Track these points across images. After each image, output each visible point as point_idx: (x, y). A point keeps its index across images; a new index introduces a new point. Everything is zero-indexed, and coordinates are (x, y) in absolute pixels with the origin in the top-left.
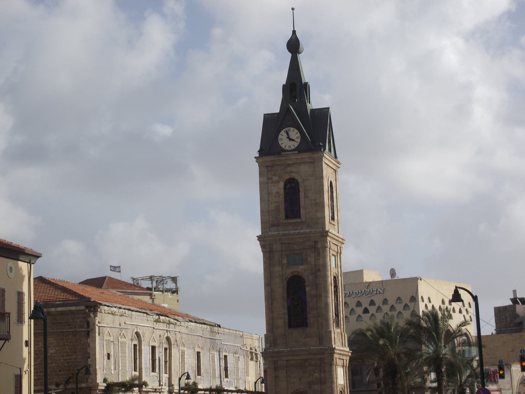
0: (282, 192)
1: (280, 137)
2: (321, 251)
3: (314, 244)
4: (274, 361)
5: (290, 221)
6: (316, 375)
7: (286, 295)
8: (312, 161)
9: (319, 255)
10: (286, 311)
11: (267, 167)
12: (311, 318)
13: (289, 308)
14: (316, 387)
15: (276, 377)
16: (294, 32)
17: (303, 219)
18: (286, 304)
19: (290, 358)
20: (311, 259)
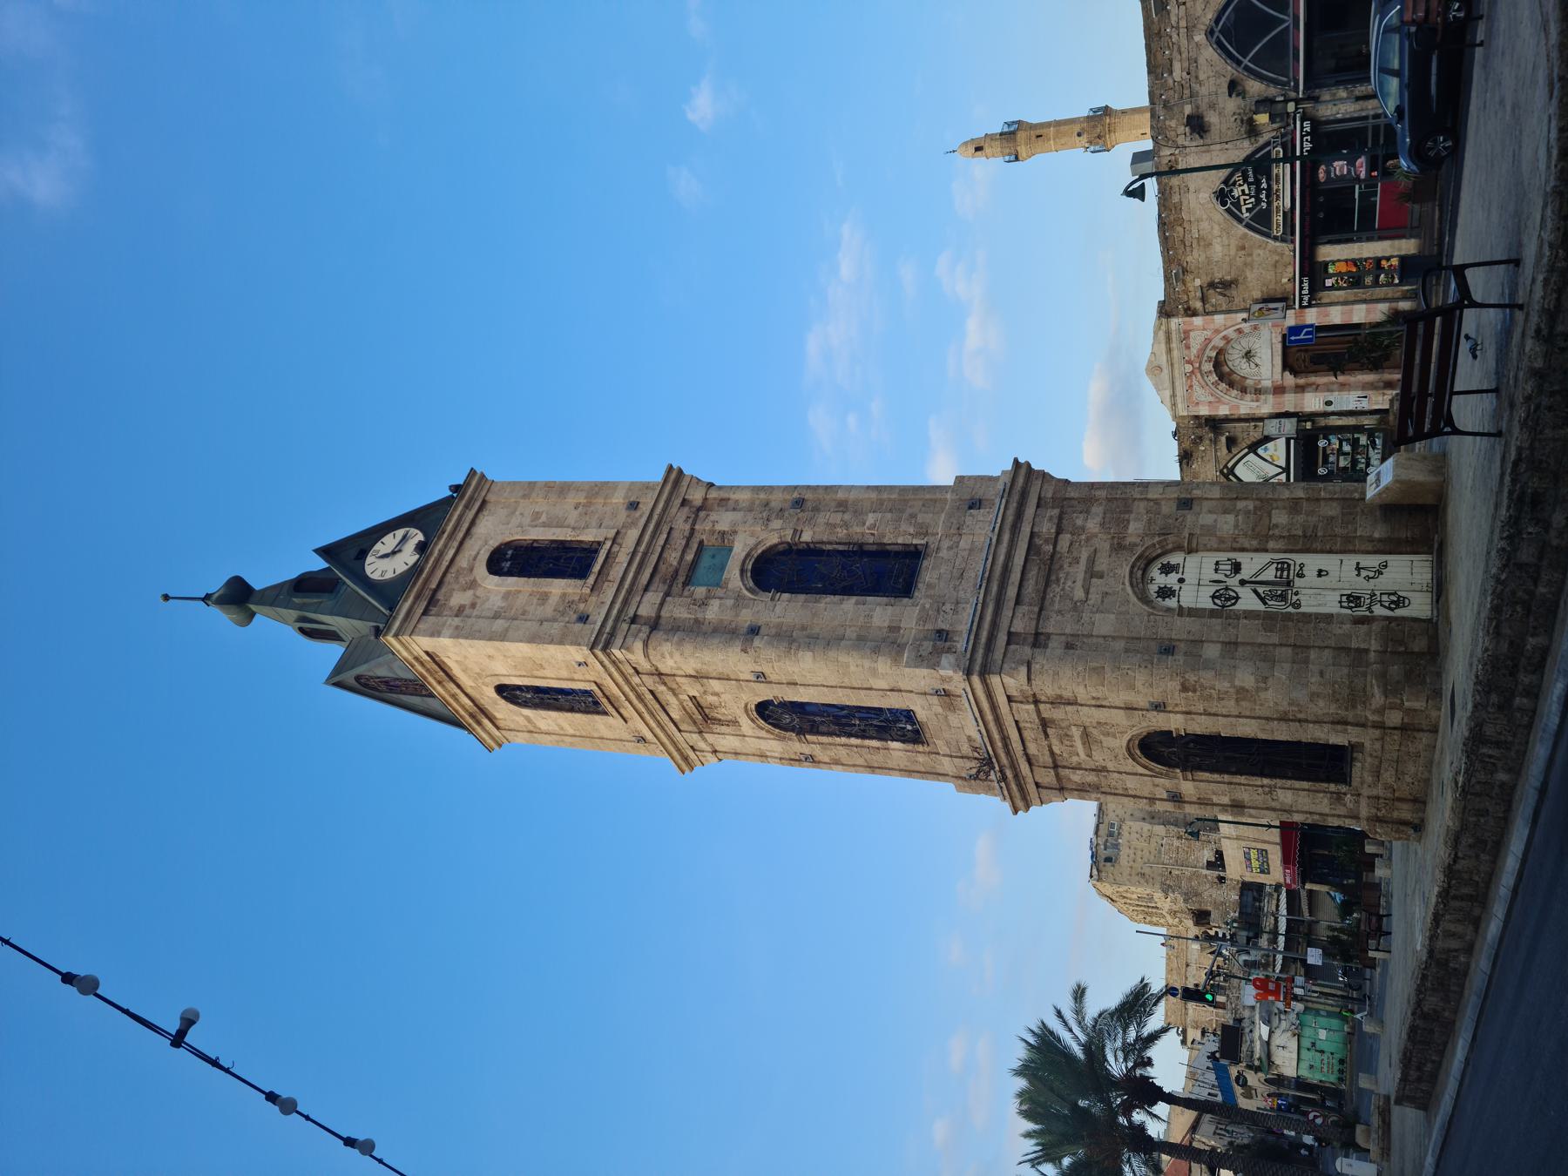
0: (512, 583)
1: (376, 576)
2: (713, 494)
3: (686, 509)
4: (1008, 643)
5: (596, 568)
6: (1093, 525)
7: (802, 597)
8: (477, 504)
9: (723, 502)
10: (854, 599)
11: (425, 613)
12: (898, 535)
13: (847, 591)
14: (1135, 528)
15: (1069, 646)
16: (207, 598)
17: (612, 533)
18: (830, 598)
19: (1012, 592)
20: (724, 520)
